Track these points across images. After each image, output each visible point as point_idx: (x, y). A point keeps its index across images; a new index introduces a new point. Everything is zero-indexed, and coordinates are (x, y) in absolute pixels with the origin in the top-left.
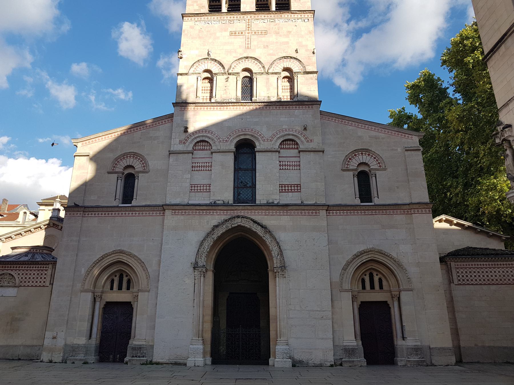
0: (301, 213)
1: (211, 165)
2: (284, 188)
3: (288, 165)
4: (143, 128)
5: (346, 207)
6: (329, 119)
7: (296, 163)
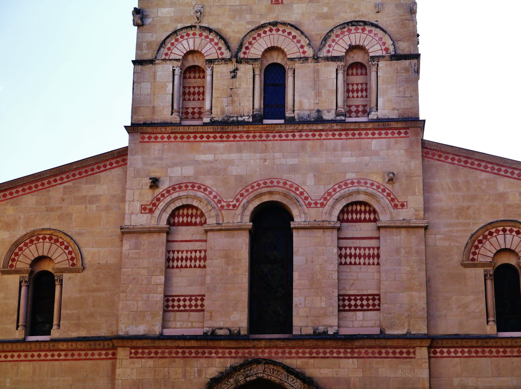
0: (380, 353)
1: (205, 256)
2: (347, 303)
3: (355, 256)
4: (68, 177)
5: (467, 340)
6: (440, 156)
7: (371, 251)
